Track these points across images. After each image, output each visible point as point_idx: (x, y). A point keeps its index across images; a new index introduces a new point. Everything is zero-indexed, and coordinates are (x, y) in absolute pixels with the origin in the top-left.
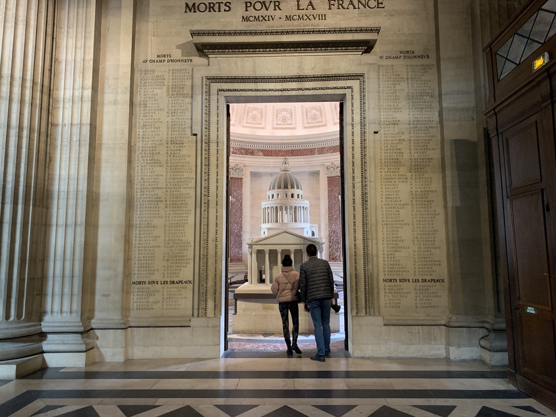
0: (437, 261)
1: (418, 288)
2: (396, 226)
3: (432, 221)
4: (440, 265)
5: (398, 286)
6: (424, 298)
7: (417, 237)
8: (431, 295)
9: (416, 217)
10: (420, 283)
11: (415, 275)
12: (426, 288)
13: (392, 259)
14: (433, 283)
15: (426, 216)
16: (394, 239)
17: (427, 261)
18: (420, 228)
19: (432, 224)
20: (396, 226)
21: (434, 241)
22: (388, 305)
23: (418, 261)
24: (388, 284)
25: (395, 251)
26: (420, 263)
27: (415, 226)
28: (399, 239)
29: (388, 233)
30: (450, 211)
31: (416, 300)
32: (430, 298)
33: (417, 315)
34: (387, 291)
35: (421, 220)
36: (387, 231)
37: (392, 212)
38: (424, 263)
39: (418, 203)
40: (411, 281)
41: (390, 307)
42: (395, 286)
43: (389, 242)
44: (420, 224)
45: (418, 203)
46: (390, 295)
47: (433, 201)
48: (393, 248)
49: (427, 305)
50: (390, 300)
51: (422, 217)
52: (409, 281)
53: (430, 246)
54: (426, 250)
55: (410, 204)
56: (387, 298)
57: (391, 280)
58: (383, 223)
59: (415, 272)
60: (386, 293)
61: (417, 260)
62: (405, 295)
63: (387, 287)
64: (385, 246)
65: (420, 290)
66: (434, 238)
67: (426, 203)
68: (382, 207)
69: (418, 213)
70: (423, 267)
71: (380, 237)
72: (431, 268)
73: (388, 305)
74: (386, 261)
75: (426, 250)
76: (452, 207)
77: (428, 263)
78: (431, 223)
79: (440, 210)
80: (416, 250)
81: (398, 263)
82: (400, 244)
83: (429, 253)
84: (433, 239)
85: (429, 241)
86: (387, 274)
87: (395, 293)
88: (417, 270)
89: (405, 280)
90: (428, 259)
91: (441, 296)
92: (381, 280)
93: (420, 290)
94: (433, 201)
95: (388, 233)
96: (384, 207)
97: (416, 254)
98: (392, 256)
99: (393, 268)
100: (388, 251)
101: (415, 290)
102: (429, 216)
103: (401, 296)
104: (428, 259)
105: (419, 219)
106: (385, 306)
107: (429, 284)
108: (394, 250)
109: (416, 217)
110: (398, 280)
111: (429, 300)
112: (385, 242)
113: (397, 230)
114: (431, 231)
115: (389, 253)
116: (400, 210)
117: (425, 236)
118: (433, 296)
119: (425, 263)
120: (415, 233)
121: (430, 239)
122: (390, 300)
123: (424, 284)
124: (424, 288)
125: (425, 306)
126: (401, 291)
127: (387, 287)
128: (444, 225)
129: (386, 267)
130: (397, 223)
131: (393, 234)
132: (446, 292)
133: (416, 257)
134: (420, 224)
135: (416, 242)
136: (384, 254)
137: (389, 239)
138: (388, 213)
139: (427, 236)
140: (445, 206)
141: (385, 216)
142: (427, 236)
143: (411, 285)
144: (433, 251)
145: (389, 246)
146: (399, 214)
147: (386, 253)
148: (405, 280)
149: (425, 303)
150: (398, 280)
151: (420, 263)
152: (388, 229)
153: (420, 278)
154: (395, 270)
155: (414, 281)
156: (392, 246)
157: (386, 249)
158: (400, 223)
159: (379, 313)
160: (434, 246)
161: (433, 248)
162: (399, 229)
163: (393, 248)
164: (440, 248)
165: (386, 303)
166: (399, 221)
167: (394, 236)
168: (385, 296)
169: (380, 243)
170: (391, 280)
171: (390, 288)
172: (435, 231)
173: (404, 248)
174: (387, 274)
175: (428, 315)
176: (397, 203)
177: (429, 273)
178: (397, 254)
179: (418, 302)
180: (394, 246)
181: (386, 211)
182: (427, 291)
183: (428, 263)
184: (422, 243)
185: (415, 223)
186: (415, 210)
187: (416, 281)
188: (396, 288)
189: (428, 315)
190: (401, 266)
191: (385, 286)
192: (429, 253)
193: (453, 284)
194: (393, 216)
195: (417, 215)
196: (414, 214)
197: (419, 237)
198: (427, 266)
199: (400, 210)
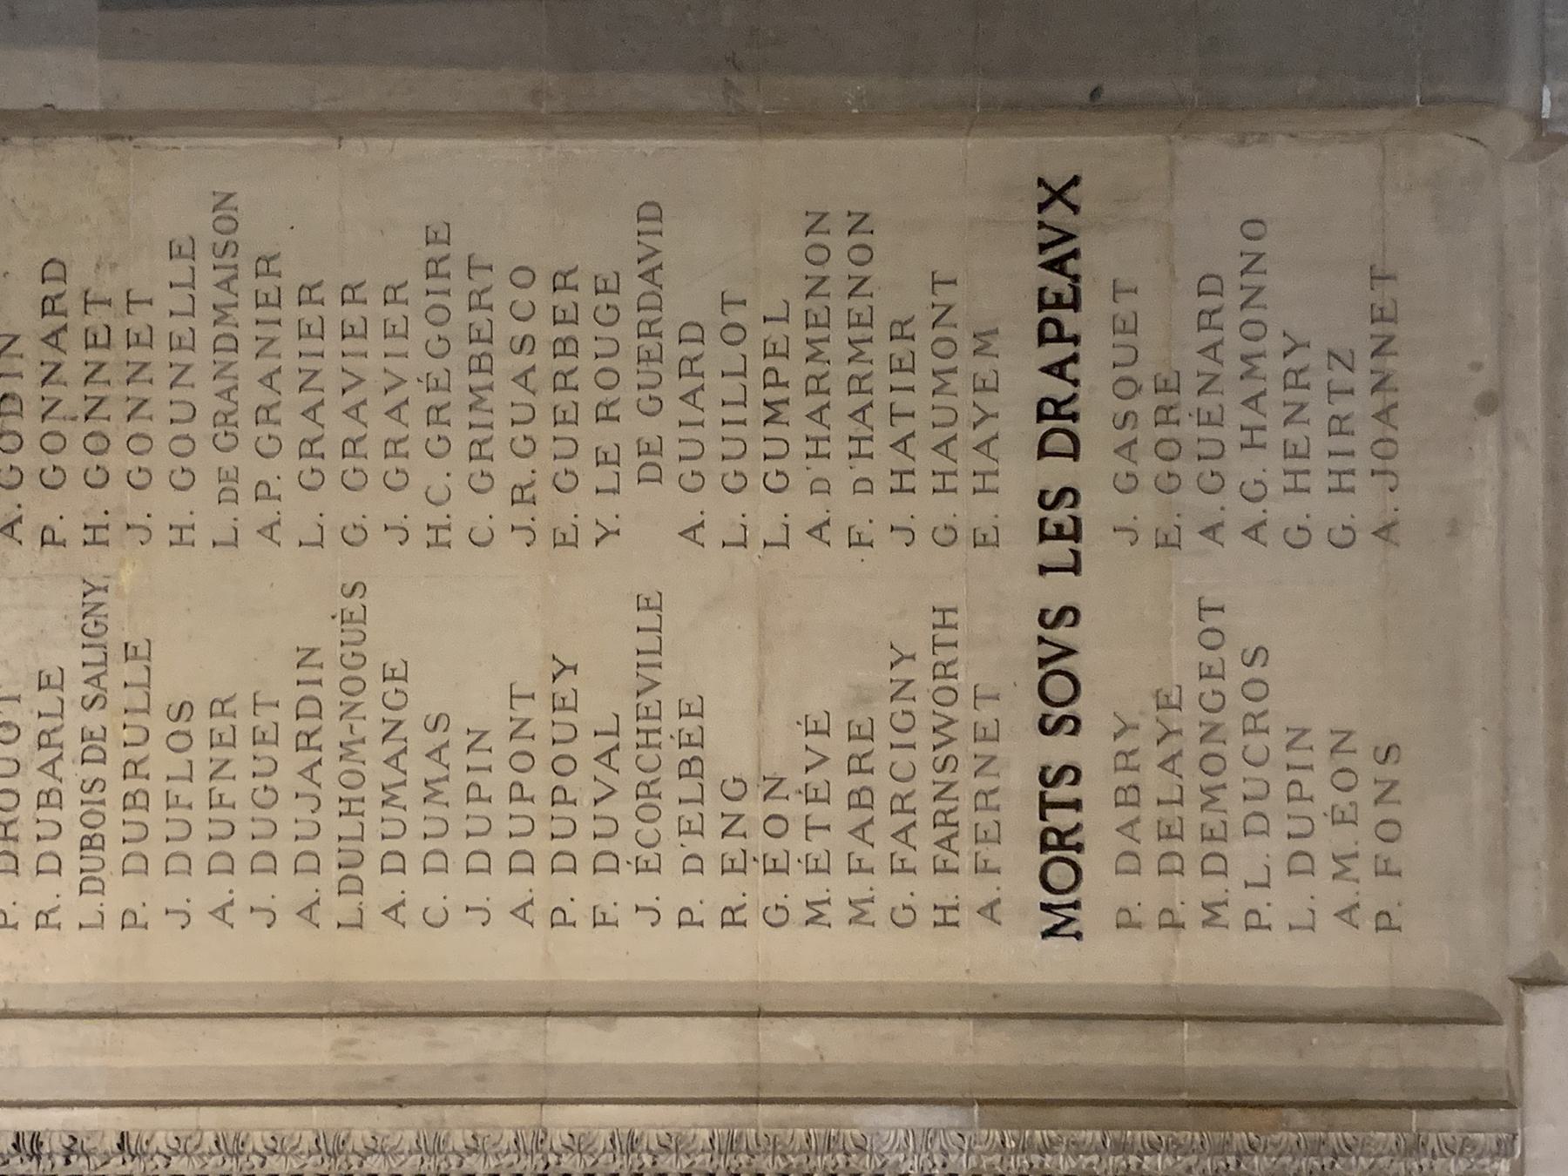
0: (817, 256)
1: (1145, 506)
2: (373, 753)
3: (308, 293)
4: (859, 222)
5: (1125, 760)
6: (1275, 435)
7: (521, 495)
8: (1234, 344)
9: (264, 491)
10: (1093, 472)
11: (980, 541)
12: (1145, 405)
13: (794, 808)
14: (1084, 322)
15: (247, 366)
16: (539, 782)
17: (815, 384)
18: (393, 447)
19: (350, 293)
20: (373, 753)
21: (561, 281)
22: (1374, 894)
23: (821, 487)
24: (1102, 885)
25: (691, 768)
26: (837, 469)
27: (378, 507)
28: (539, 713)
29: (459, 848)
30: (151, 83)
31: (1299, 538)
32: (1273, 366)
33: (1482, 539)
34: (1192, 890)
35: (292, 427)
36: (437, 862)
37: (194, 792)
38: (840, 427)
39: (74, 460)
40: (1058, 590)
41: (1386, 871)
42: (1127, 797)
43: (584, 846)
44: (350, 448)
45: (74, 460)
46: (1243, 854)
47: (53, 269)
48: (647, 793)
49: (1362, 405)
50: (1299, 865)
51: (263, 414)
52: (1069, 614)
53: (625, 331)
54: (672, 389)
55: (96, 563)
56: (1281, 901)
57: (1060, 844)
58: (344, 907)
59: (946, 536)
60: (1212, 914)
61: (807, 509)
62: (1237, 673)
63: (1148, 891)
64: (624, 889)
65: (1168, 486)
66: (523, 275)
67: (75, 361)
68: (130, 920)
69: (206, 461)
70: (884, 434)
71: (507, 956)
72: (900, 331)
73: (1374, 894)
74: (813, 887)
75: (672, 389)
76: (110, 50)
77: (840, 371)
78: (334, 312)
79: (173, 186)
80: (689, 508)
81: (838, 747)
82: (602, 700)
83: (716, 355)
84: (540, 292)
85: (564, 348)
86: (975, 890)
87: (1210, 797)
88: (926, 509)
89: (1055, 660)
90: (795, 370)
91: (1253, 227)
92: (1054, 967)
93: (1168, 486)
94: (53, 269)
95: (459, 848)
96: (120, 894)
97: (721, 511)
98: (754, 808)
99: (900, 804)
100: (693, 864)
101: (1166, 542)
102: (247, 333)
103: (1253, 725)
104: (795, 370)
105: (286, 466)
106: (1385, 921)
107: (1093, 369)
108: (672, 788)
109: (264, 491)
110: (1059, 750)
111: (1294, 379)
112: (581, 890)
113: (421, 742)
114: (438, 316)
115: (711, 845)
116: (162, 695)
117: (504, 393)
118: (1254, 330)
119: (842, 402)
120: (468, 511)
121: (543, 329)
122: (1299, 865)
123: (1093, 426)
124: (1147, 434)
125: (1367, 430)
126: (1189, 720)
127: (1148, 891)
128: (353, 144)
129: (891, 891)
130: (332, 731)
131: (474, 793)
132: (1208, 155)
133: (764, 512)
134: (350, 448)
135: (585, 507)
136: (731, 917)
137: (541, 846)
138: (199, 849)
139: (508, 364)
140: (112, 125)
141: (247, 889)
142: (508, 364)
143: (1108, 586)
144: (686, 299)
145: (625, 847)
146: (219, 706)
147: (714, 890)
148: (1055, 660)
149: (1339, 426)
150: (1059, 750)
151: (837, 469)
152: (413, 847)
153: (1022, 476)
154: (925, 784)
155: (1059, 551)
156: (623, 807)
157: (672, 889)
158: (329, 694)
159: (1472, 1013)
160: (633, 287)
161: (651, 303)
162: (412, 718)
163: (647, 793)
164: (650, 213)
165: (1346, 914)
166: (308, 707)
167: (497, 783)
168: (1254, 922)
169: (586, 960)
170: (1060, 844)
171: (1151, 848)
172: (433, 268)
173: (649, 659)
174: (975, 890)
175: (1490, 403)
176: (75, 720)
177: (964, 361)
178: (731, 750)
179: (1321, 508)
180: (628, 777)
181: (178, 864)
182: (1189, 399)
183: (840, 371)
184: (590, 433)
185: (340, 507)
186: (164, 504)
187: (1060, 523)
188: (1154, 781)
189: (1490, 403)
190: (882, 710)
191: (1126, 921)
192: (716, 355)
193: (1115, 89)
194: (238, 789)
195: (228, 483)
196: (211, 520)
197: (509, 470)
198: (881, 380)
199: (162, 695)
